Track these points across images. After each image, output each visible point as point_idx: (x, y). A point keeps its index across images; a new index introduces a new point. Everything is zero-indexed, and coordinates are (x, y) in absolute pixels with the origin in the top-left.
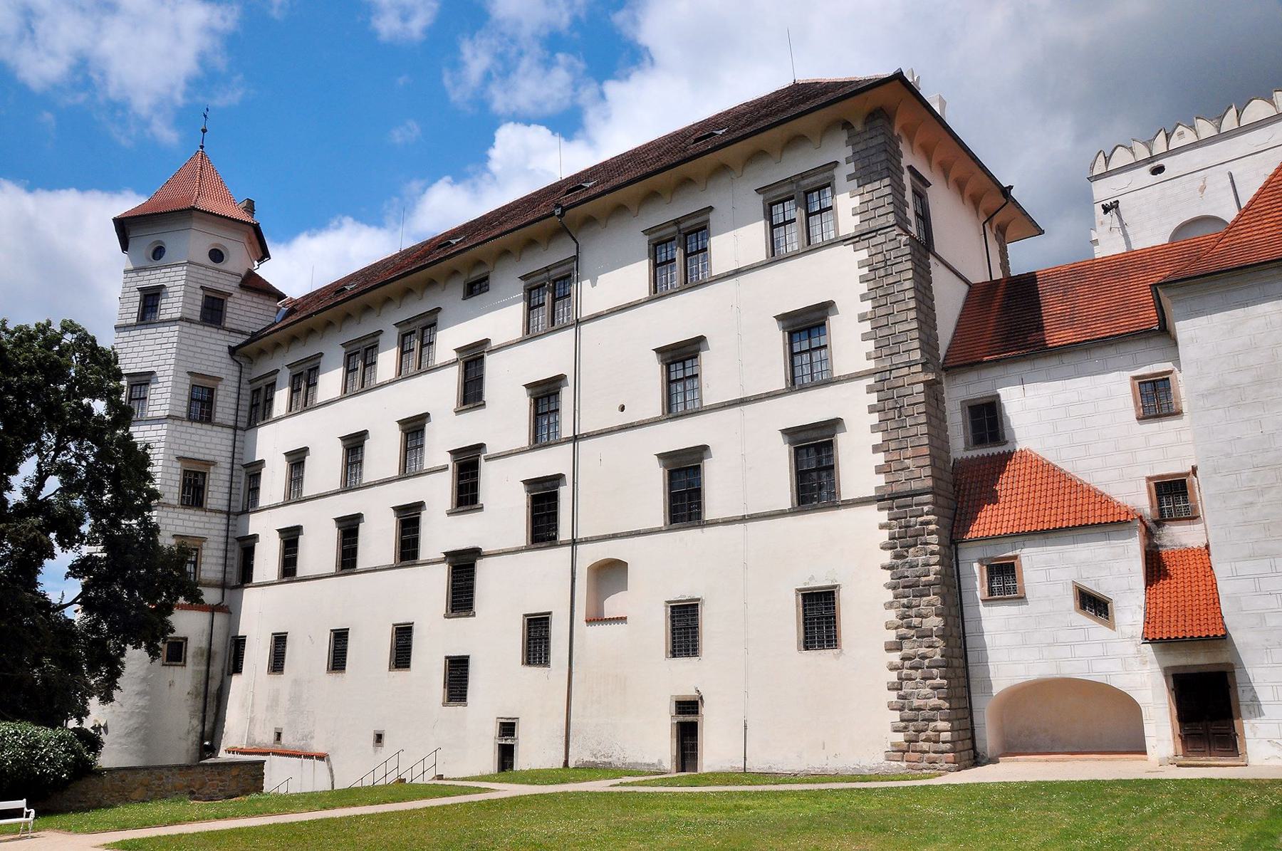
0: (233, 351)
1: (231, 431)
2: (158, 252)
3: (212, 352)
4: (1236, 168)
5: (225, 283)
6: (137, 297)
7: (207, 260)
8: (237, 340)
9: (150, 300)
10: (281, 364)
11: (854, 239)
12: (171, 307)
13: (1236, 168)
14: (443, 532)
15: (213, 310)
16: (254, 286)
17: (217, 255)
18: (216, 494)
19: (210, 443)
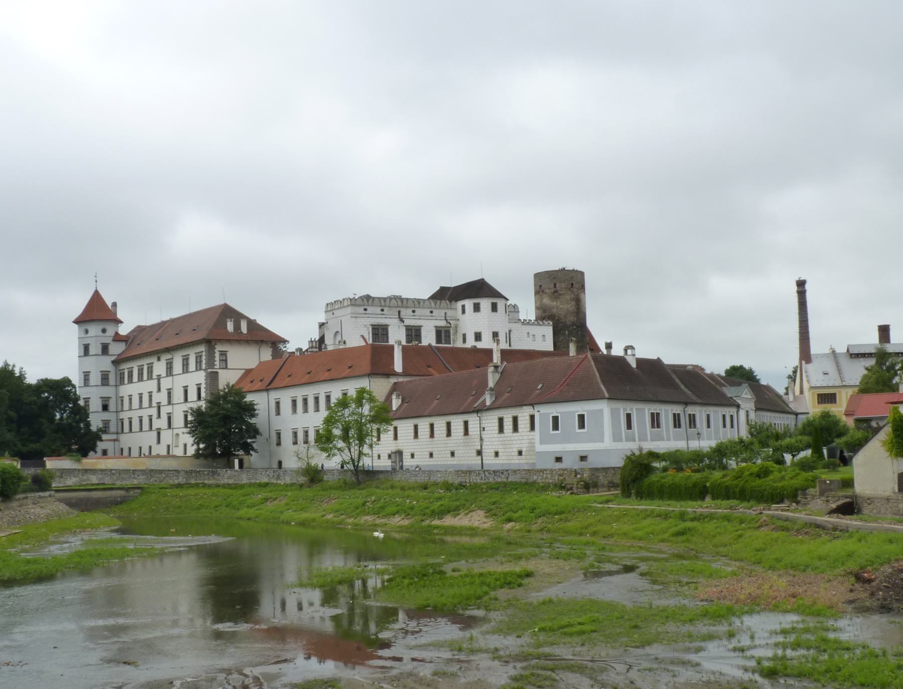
0: (113, 362)
1: (114, 388)
2: (87, 332)
3: (106, 363)
4: (342, 318)
5: (108, 340)
6: (83, 347)
7: (102, 334)
8: (113, 358)
9: (86, 348)
10: (125, 367)
11: (205, 370)
12: (92, 351)
13: (342, 318)
14: (156, 424)
15: (105, 349)
16: (117, 338)
17: (104, 331)
18: (112, 407)
19: (108, 391)
